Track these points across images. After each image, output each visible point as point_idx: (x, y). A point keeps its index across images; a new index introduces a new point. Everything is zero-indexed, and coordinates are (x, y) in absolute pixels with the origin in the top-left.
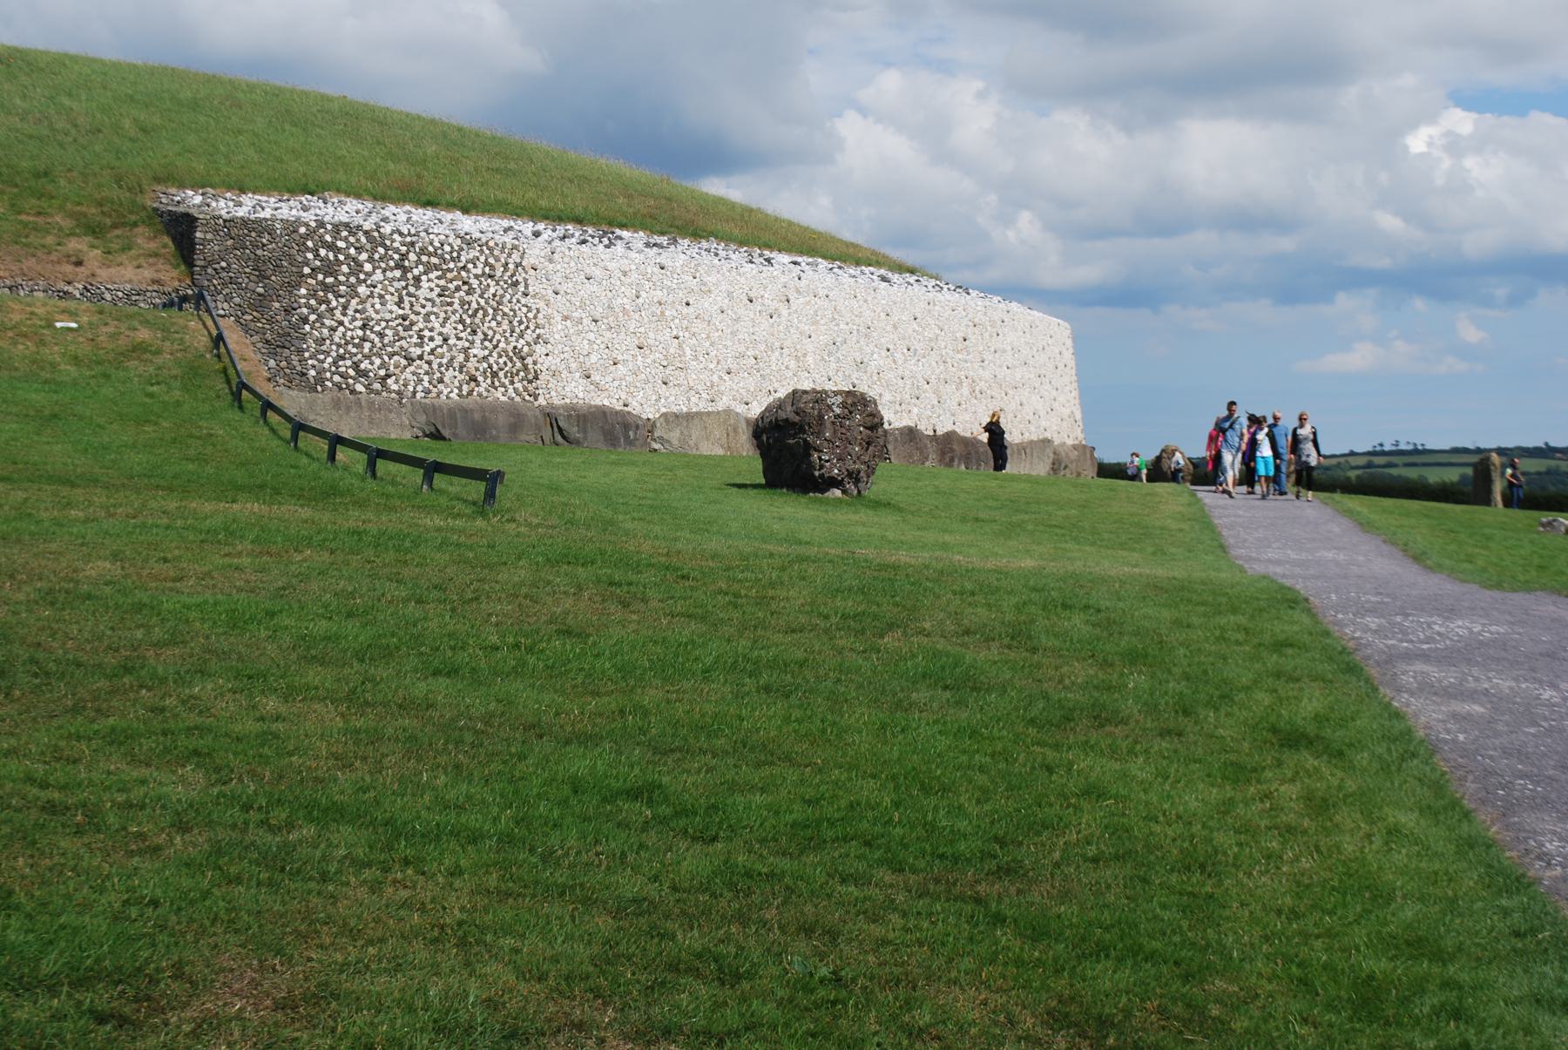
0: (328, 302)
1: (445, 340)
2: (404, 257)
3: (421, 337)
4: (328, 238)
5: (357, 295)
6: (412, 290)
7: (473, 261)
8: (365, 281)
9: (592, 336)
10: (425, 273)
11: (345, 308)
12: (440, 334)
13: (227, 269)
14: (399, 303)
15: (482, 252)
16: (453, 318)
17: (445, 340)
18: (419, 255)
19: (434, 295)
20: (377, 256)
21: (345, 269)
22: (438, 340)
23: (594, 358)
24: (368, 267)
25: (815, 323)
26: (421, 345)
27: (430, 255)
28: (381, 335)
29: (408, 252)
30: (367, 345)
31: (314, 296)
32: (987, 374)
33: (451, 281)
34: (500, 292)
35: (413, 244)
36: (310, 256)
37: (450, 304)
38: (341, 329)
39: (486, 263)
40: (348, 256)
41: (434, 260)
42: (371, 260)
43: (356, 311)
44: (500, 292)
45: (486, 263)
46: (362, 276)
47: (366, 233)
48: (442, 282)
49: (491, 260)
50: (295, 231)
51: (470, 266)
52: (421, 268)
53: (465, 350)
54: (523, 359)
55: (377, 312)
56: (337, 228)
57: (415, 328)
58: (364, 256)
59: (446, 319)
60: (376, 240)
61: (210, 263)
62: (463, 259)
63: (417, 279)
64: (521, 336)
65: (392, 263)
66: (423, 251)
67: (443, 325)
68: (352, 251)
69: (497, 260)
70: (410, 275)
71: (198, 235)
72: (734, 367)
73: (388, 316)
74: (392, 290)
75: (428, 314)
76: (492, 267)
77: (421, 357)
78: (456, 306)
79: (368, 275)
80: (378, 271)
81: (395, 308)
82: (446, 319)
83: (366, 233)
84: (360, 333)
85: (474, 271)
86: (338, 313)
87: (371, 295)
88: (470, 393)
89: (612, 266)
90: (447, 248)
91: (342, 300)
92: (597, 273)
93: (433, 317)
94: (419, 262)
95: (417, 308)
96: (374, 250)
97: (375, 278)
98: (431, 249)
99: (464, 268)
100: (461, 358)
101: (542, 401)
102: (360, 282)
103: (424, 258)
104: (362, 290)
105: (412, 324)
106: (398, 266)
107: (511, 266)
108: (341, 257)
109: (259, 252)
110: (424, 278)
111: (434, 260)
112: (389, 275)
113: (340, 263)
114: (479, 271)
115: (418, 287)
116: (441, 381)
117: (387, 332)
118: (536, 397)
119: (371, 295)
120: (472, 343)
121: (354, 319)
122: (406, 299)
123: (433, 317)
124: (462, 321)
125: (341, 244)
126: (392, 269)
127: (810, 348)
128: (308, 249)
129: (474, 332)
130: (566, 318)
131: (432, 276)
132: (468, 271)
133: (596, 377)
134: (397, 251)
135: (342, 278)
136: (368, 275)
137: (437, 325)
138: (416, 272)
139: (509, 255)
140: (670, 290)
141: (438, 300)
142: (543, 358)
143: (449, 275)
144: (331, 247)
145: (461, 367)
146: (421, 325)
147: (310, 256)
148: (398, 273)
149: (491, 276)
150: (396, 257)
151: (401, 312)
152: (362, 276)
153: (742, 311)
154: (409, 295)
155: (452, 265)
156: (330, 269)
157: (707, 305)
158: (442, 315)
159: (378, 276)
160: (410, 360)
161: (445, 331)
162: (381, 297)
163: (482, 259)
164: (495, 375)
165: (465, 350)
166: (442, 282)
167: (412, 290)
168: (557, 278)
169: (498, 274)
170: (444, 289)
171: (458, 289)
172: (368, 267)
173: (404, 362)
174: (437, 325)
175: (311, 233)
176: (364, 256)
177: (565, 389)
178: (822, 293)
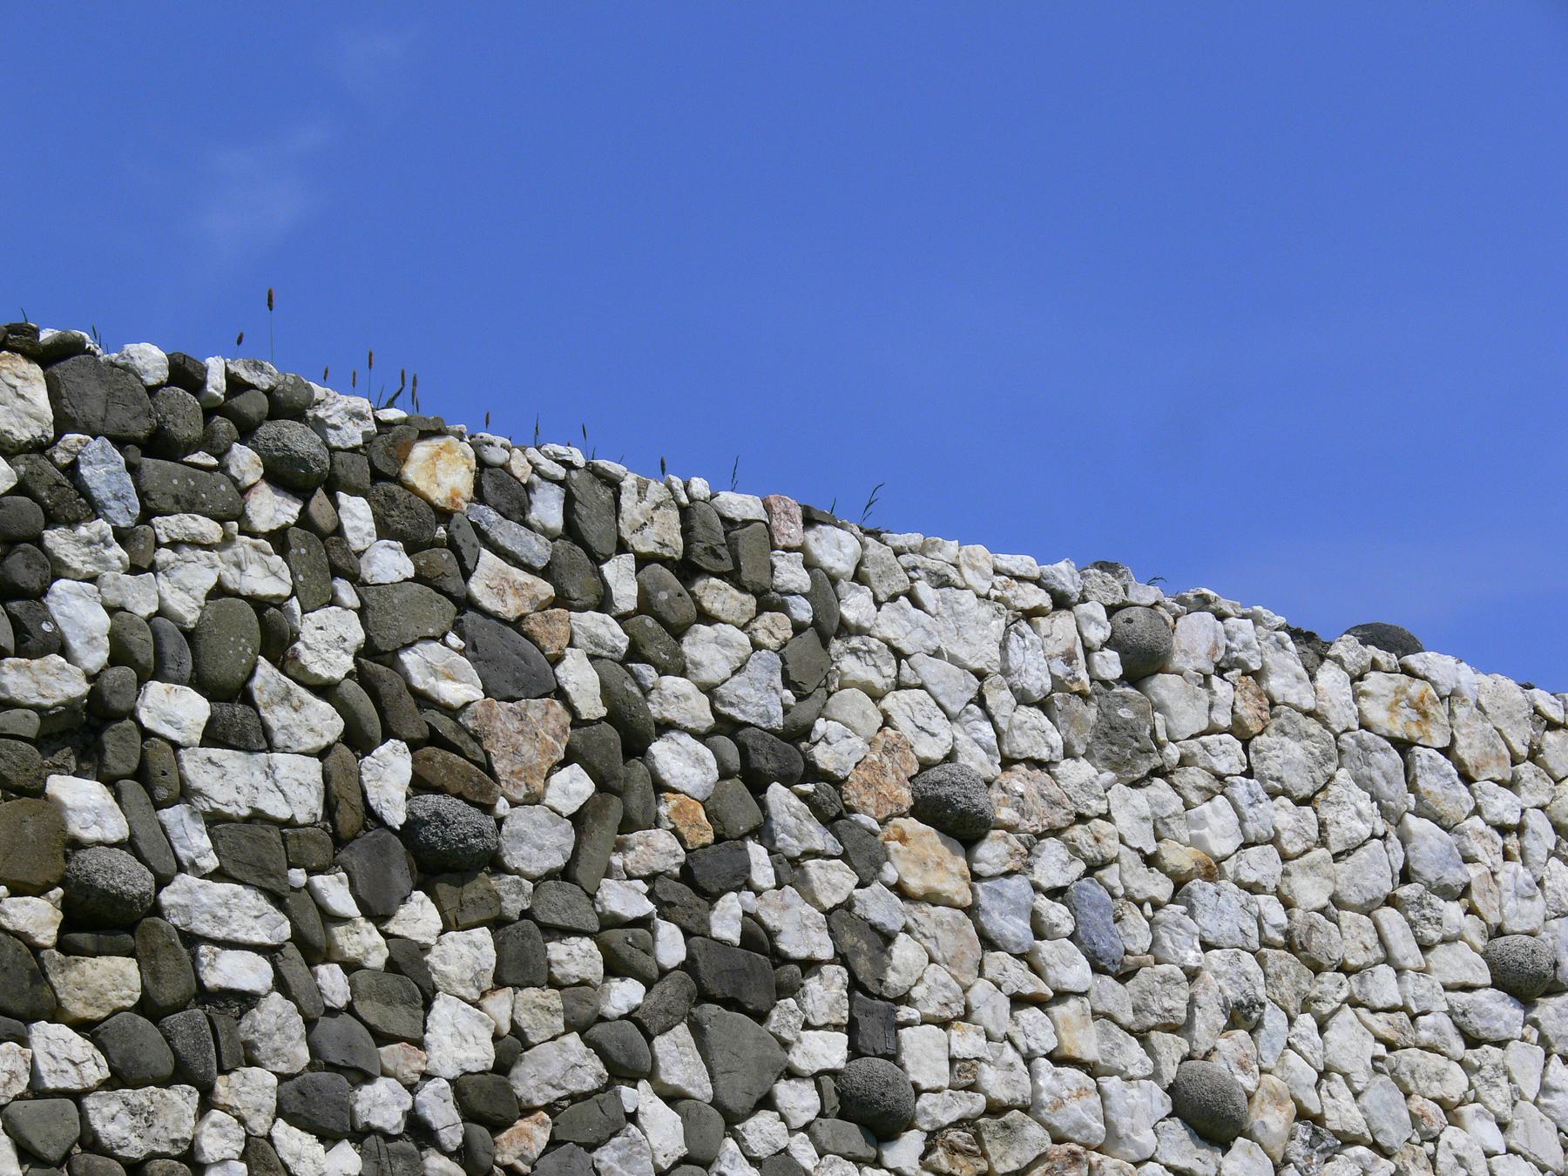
7: (229, 661)
15: (323, 557)
34: (560, 1065)
39: (376, 700)
44: (560, 1065)
49: (442, 672)
51: (175, 709)
62: (77, 611)
69: (519, 669)
76: (440, 739)
85: (228, 780)
107: (684, 764)
114: (291, 788)
132: (149, 777)
139: (659, 633)
163: (329, 639)
169: (536, 842)
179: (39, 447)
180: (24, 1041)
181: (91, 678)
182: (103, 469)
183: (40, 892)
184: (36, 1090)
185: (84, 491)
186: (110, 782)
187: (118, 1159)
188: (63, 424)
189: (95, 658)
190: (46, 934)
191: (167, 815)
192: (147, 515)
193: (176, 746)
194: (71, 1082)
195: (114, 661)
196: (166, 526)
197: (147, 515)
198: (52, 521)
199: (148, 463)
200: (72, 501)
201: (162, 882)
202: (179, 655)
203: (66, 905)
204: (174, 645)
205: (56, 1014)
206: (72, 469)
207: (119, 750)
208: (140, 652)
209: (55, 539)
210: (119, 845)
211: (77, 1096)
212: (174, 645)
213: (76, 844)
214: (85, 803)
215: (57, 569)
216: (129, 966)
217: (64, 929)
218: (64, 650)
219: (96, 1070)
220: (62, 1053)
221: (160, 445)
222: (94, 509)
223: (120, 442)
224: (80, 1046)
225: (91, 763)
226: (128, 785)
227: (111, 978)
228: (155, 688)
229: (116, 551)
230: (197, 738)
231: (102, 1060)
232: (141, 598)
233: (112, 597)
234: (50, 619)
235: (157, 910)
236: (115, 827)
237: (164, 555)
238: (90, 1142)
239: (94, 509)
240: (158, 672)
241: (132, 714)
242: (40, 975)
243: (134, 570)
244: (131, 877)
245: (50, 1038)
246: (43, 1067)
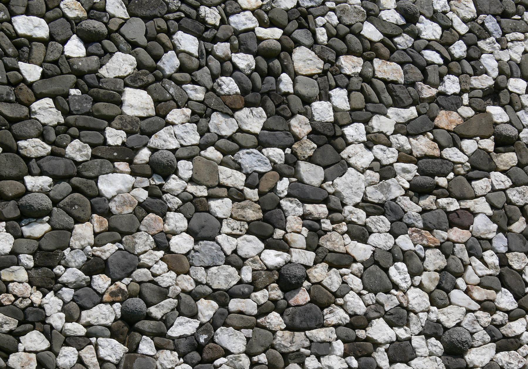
5: (99, 205)
6: (311, 174)
8: (127, 153)
10: (356, 115)
11: (47, 258)
12: (434, 330)
14: (267, 227)
16: (476, 271)
20: (170, 63)
21: (46, 111)
24: (137, 102)
27: (369, 52)
29: (288, 46)
33: (456, 138)
37: (461, 219)
38: (35, 340)
40: (57, 67)
41: (387, 70)
42: (147, 76)
43: (94, 266)
46: (115, 137)
48: (423, 145)
52: (340, 97)
55: (178, 264)
57: (336, 315)
59: (449, 277)
62: (489, 62)
63: (329, 137)
65: (229, 85)
66: (345, 38)
68: (75, 48)
70: (300, 126)
73: (224, 277)
74: (234, 178)
75: (379, 262)
78: (483, 225)
79: (142, 129)
80: (176, 115)
81: (250, 245)
82: (449, 277)
87: (156, 203)
90: (430, 30)
91: (39, 229)
93: (399, 273)
94: (330, 77)
95: (337, 241)
96: (158, 42)
97: (165, 140)
98: (370, 31)
99: (495, 94)
102: (106, 157)
103: (351, 65)
104: (115, 184)
105: (324, 299)
108: (32, 72)
110: (355, 131)
111: (387, 70)
112: (221, 124)
115: (338, 166)
119: (156, 203)
122: (293, 209)
123: (399, 273)
131: (383, 124)
134: (242, 41)
135: (34, 147)
136: (142, 129)
137: (417, 299)
138: (322, 111)
141: (412, 208)
143: (446, 120)
146: (356, 304)
148: (253, 120)
150: (244, 61)
151: (273, 258)
152: (115, 137)
154: (302, 194)
155: (452, 85)
158: (434, 259)
159: (179, 132)
161: (449, 317)
162: (195, 206)
166: (423, 145)
167: (311, 174)
171: (481, 165)
172: (137, 102)
174: (417, 299)
176: (121, 64)
179: (473, 20)
180: (489, 177)
181: (494, 79)
182: (491, 23)
183: (488, 137)
184: (493, 190)
185: (487, 30)
186: (503, 106)
187: (517, 206)
188: (479, 13)
189: (495, 74)
190: (491, 149)
191: (519, 113)
192: (504, 34)
193: (519, 95)
194: (502, 187)
195: (500, 74)
196: (509, 36)
197: (504, 34)
198: (479, 39)
199: (503, 20)
200: (483, 33)
201: (520, 131)
202: (517, 70)
203: (495, 140)
204: (515, 68)
205: (496, 169)
206: (483, 25)
207: (504, 97)
208: (506, 71)
209: (481, 43)
210: (507, 123)
211: (504, 190)
212: (515, 68)
213: (496, 124)
214: (497, 113)
215: (482, 52)
216: (513, 155)
217: (496, 146)
218: (486, 73)
219: (508, 183)
220: (499, 179)
221: (505, 15)
222: (490, 34)
223: (494, 16)
224: (503, 177)
225: (497, 102)
226: (508, 107)
227: (509, 158)
228: (512, 80)
229: (497, 45)
230: (524, 92)
231: (510, 180)
232: (505, 56)
233: (498, 57)
234: (482, 65)
235: (519, 139)
236: (506, 118)
237: (510, 44)
238: (509, 202)
239: (490, 34)
240: (512, 76)
241: (506, 88)
242: (491, 159)
243: (502, 49)
244: (511, 131)
245: (495, 175)
246: (495, 183)
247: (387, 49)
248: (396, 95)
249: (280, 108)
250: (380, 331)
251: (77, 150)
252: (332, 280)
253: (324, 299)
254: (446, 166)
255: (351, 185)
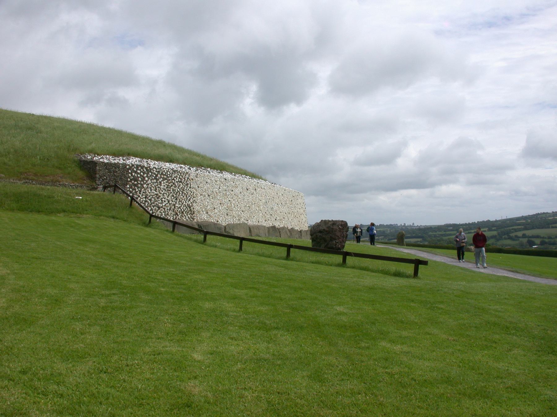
0: (135, 190)
1: (169, 202)
2: (157, 175)
3: (162, 201)
4: (135, 169)
9: (208, 200)
11: (140, 191)
13: (106, 179)
14: (156, 190)
17: (169, 202)
18: (161, 175)
19: (165, 188)
21: (140, 179)
22: (167, 202)
23: (209, 207)
24: (146, 179)
25: (262, 196)
26: (162, 203)
27: (164, 175)
28: (150, 200)
30: (147, 203)
31: (131, 188)
32: (296, 211)
35: (159, 172)
36: (130, 175)
39: (179, 178)
40: (141, 175)
41: (165, 177)
42: (147, 176)
45: (179, 178)
47: (146, 168)
50: (126, 167)
53: (174, 205)
54: (190, 207)
56: (138, 166)
58: (145, 175)
59: (169, 195)
60: (149, 170)
61: (101, 177)
63: (160, 182)
64: (189, 200)
66: (162, 174)
67: (168, 197)
71: (97, 168)
72: (244, 210)
73: (152, 194)
75: (164, 194)
77: (162, 207)
79: (147, 181)
82: (169, 195)
83: (146, 168)
84: (145, 199)
86: (138, 193)
87: (148, 188)
88: (176, 218)
89: (213, 179)
92: (209, 181)
95: (161, 192)
96: (148, 174)
97: (148, 182)
99: (173, 179)
100: (173, 207)
101: (195, 220)
103: (162, 176)
105: (159, 196)
106: (155, 178)
109: (115, 174)
111: (165, 177)
112: (153, 181)
113: (139, 177)
115: (161, 185)
116: (168, 214)
117: (153, 199)
118: (194, 219)
119: (148, 188)
120: (176, 202)
121: (143, 195)
124: (173, 196)
125: (139, 171)
126: (153, 179)
127: (261, 204)
128: (129, 173)
129: (176, 199)
130: (201, 195)
131: (165, 182)
133: (210, 213)
134: (155, 174)
135: (139, 182)
140: (228, 186)
142: (196, 207)
144: (136, 172)
145: (173, 210)
147: (130, 175)
148: (155, 181)
149: (181, 182)
153: (245, 193)
154: (158, 187)
156: (136, 179)
157: (237, 191)
159: (149, 182)
160: (159, 208)
162: (151, 188)
164: (182, 212)
165: (174, 205)
168: (199, 183)
170: (168, 186)
171: (172, 186)
172: (146, 179)
173: (157, 208)
175: (130, 168)
176: (145, 175)
177: (202, 217)
178: (263, 187)
247: (165, 175)
248: (166, 179)
249: (157, 180)
250: (163, 199)
251: (142, 183)
252: (160, 194)
253: (159, 196)
254: (168, 186)
255: (162, 187)
